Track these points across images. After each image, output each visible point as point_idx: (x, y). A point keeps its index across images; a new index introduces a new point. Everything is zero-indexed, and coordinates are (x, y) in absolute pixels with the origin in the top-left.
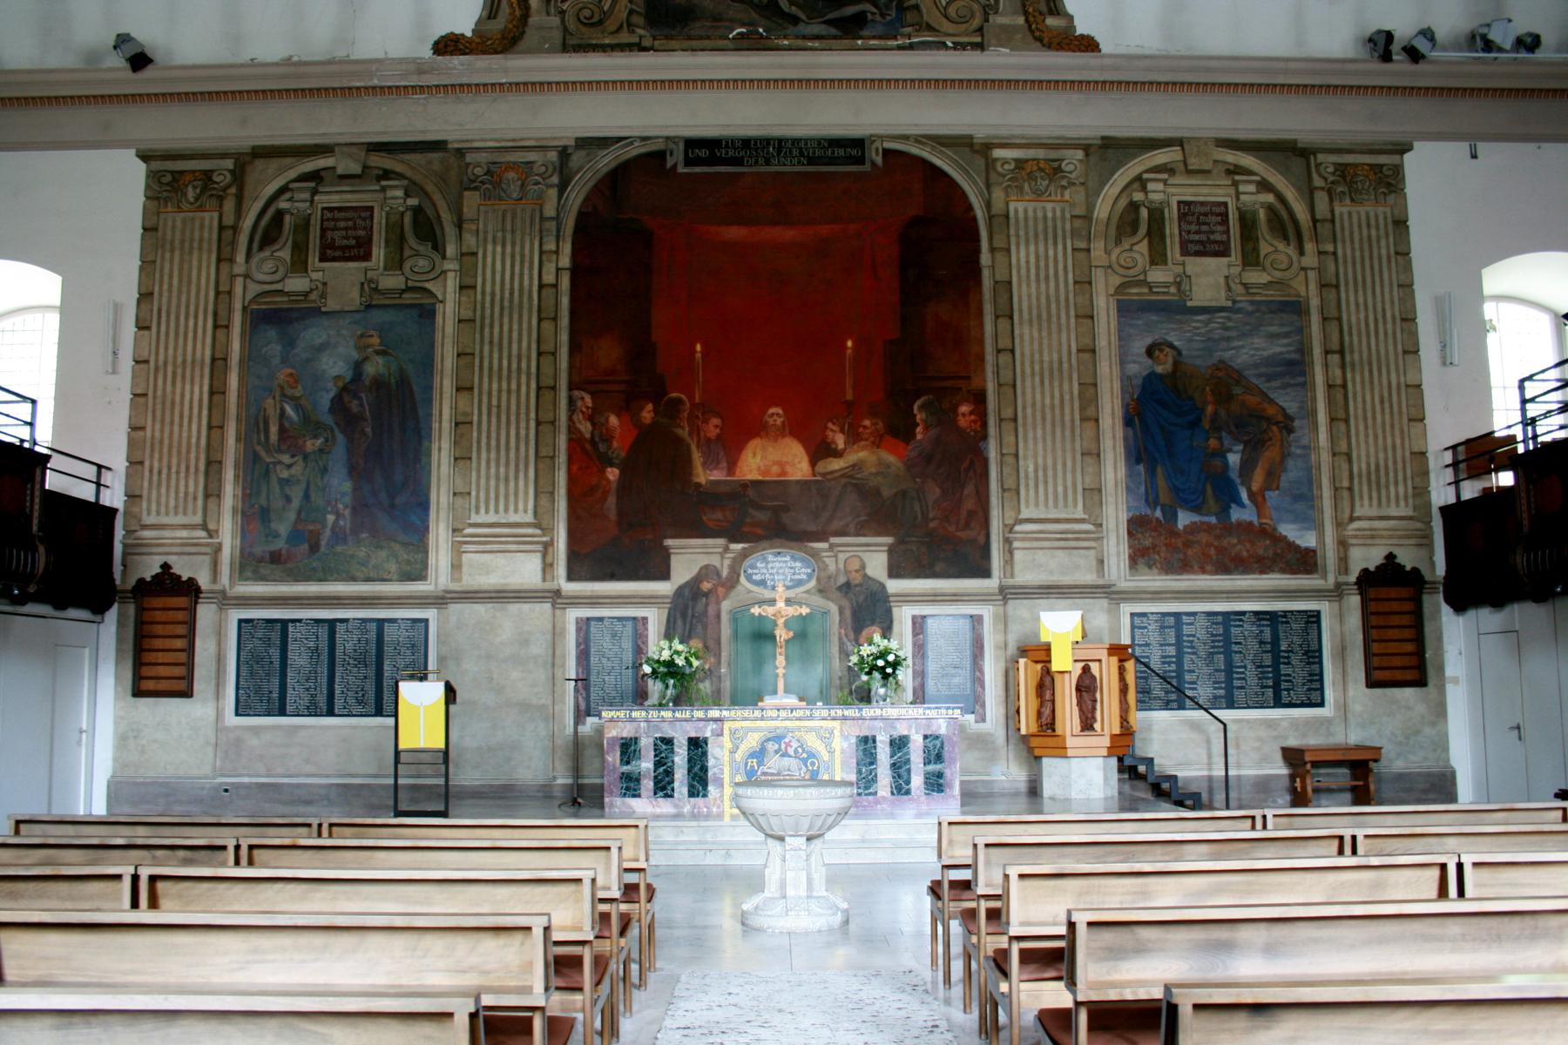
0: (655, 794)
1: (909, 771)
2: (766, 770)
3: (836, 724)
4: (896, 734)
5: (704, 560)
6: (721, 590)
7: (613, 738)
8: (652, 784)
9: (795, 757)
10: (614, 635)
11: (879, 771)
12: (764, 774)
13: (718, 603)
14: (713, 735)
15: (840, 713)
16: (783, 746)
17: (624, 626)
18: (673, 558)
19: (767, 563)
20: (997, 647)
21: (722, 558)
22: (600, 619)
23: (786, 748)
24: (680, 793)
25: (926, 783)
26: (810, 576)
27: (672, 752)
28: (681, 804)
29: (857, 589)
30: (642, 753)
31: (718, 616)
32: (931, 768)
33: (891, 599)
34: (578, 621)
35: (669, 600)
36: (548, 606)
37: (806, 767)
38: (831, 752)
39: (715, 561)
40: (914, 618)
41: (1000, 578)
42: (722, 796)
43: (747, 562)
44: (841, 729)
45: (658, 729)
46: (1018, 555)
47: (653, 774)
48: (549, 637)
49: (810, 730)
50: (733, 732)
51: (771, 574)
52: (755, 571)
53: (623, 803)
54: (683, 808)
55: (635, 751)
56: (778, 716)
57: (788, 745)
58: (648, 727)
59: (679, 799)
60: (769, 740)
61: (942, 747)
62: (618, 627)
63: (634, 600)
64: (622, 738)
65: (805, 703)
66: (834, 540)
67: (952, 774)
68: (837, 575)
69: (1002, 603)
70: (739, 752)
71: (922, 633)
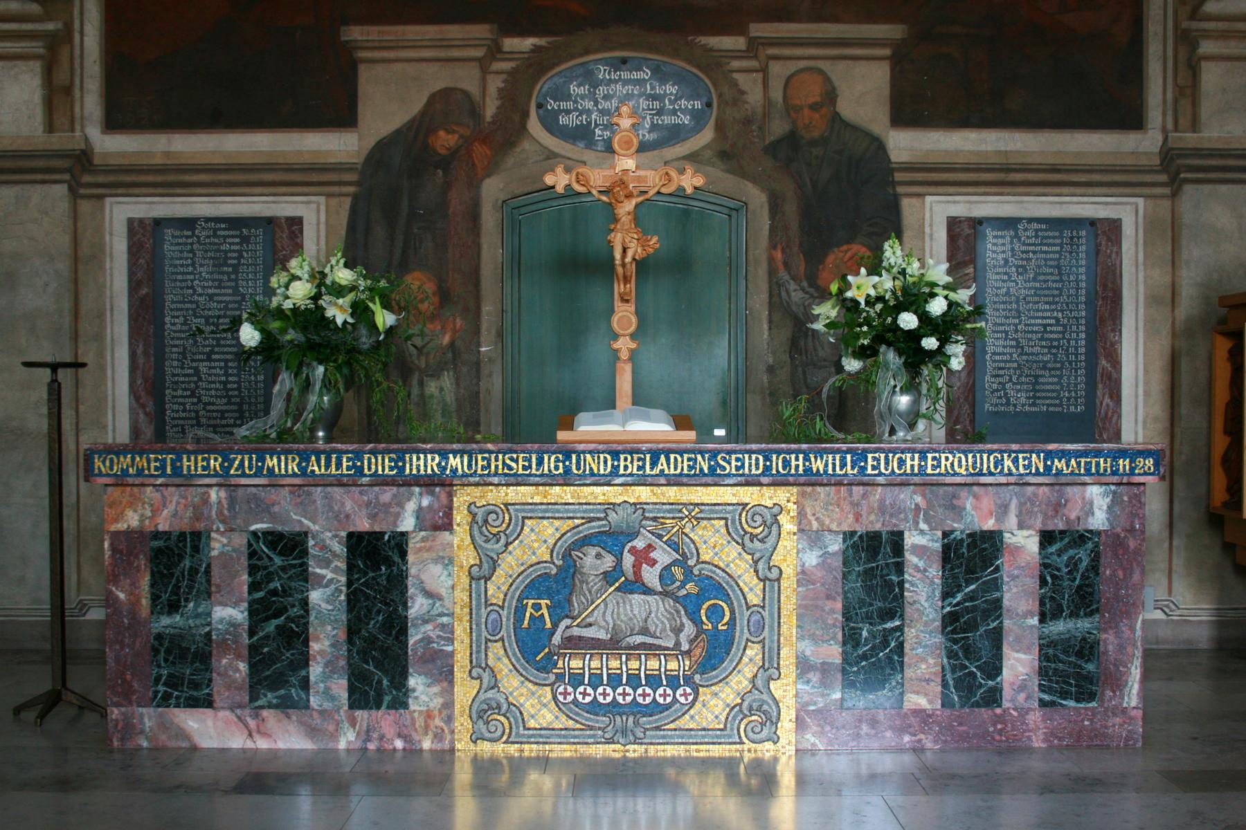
0: (253, 698)
1: (997, 638)
2: (576, 632)
3: (782, 496)
4: (959, 528)
5: (438, 79)
6: (480, 150)
7: (129, 533)
8: (243, 666)
9: (665, 594)
10: (220, 262)
11: (910, 634)
12: (572, 643)
13: (474, 184)
14: (420, 527)
15: (797, 462)
16: (628, 560)
17: (245, 240)
18: (364, 73)
19: (595, 85)
20: (1153, 300)
21: (485, 72)
22: (189, 223)
23: (637, 567)
24: (327, 693)
25: (1042, 672)
26: (699, 118)
27: (304, 575)
28: (331, 728)
29: (817, 151)
30: (216, 579)
31: (474, 216)
32: (1059, 627)
33: (898, 177)
34: (135, 228)
35: (353, 177)
36: (61, 190)
37: (697, 622)
38: (771, 581)
39: (466, 79)
40: (953, 223)
41: (1164, 130)
42: (449, 705)
43: (544, 85)
44: (801, 514)
45: (262, 508)
46: (1211, 75)
47: (246, 640)
48: (63, 266)
49: (701, 513)
50: (480, 521)
51: (603, 112)
52: (563, 105)
53: (163, 725)
54: (334, 736)
55: (194, 571)
56: (615, 472)
57: (644, 557)
58: (232, 501)
59: (322, 713)
60: (585, 541)
61: (1094, 567)
62: (231, 244)
63: (269, 177)
64: (157, 535)
65: (691, 435)
66: (759, 30)
67: (1121, 648)
68: (766, 115)
69: (1167, 191)
71: (973, 261)
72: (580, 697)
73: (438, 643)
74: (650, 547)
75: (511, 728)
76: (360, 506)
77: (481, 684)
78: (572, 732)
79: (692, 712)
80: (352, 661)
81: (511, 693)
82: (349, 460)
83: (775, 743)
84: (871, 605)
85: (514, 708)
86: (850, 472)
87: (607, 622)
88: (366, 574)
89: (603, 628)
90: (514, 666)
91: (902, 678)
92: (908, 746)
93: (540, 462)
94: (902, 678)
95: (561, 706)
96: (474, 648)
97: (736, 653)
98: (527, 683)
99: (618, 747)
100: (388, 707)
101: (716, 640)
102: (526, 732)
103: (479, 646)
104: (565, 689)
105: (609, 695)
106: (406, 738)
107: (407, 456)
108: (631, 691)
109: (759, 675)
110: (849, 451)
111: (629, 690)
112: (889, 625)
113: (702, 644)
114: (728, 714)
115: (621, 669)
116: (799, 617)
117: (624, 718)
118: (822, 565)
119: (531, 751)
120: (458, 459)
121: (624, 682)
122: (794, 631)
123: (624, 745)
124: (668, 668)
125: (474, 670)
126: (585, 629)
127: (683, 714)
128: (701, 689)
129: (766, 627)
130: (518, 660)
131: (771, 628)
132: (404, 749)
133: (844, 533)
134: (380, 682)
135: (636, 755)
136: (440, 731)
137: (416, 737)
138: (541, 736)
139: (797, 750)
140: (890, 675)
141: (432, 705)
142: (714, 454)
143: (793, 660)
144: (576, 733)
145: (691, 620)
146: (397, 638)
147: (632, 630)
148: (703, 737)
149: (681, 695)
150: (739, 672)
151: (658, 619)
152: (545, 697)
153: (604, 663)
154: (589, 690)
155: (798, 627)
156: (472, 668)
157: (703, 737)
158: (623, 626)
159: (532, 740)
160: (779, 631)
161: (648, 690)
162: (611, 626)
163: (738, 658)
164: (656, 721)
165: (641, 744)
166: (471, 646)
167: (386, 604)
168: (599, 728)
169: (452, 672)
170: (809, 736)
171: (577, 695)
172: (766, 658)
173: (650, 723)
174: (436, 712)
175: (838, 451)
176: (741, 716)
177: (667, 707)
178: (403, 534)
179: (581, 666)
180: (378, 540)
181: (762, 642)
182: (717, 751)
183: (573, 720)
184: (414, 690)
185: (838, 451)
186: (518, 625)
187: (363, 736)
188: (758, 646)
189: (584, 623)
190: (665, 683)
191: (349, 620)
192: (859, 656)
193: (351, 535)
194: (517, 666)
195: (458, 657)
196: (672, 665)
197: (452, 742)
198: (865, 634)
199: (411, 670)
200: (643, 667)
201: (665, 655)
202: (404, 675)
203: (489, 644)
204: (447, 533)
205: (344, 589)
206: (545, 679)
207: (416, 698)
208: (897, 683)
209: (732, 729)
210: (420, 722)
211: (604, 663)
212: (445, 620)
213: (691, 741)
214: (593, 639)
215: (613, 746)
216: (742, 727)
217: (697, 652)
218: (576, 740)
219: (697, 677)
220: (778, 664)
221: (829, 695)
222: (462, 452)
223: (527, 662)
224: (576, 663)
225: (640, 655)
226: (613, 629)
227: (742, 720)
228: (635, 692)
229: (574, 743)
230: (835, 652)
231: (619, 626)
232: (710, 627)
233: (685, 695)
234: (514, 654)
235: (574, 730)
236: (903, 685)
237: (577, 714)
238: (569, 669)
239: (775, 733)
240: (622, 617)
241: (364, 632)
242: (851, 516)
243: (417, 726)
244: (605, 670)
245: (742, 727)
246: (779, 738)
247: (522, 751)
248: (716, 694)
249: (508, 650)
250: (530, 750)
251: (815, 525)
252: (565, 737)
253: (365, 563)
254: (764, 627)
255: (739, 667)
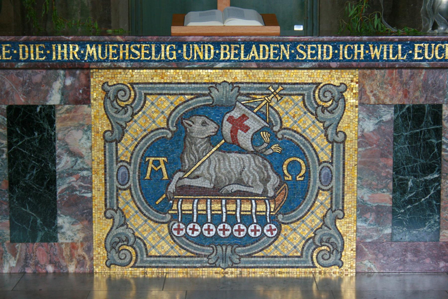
2: (187, 182)
9: (255, 153)
14: (65, 100)
16: (227, 127)
23: (234, 132)
37: (281, 175)
42: (89, 239)
44: (362, 93)
65: (276, 29)
70: (128, 138)
72: (190, 232)
73: (80, 191)
74: (244, 117)
75: (137, 256)
76: (17, 85)
77: (114, 222)
78: (184, 259)
79: (276, 243)
80: (12, 206)
81: (137, 229)
82: (7, 48)
83: (340, 267)
84: (416, 162)
85: (139, 241)
86: (400, 58)
87: (210, 175)
88: (22, 138)
89: (208, 179)
90: (139, 208)
91: (439, 218)
92: (443, 270)
93: (158, 51)
94: (439, 218)
95: (176, 239)
96: (108, 195)
97: (310, 199)
98: (149, 221)
99: (219, 269)
100: (41, 241)
101: (295, 188)
102: (148, 259)
103: (111, 193)
104: (179, 226)
105: (212, 230)
106: (55, 264)
107: (54, 46)
108: (229, 228)
109: (328, 215)
110: (400, 42)
111: (227, 226)
112: (430, 177)
113: (284, 191)
114: (304, 245)
115: (221, 210)
116: (360, 171)
117: (224, 248)
118: (377, 131)
119: (153, 273)
120: (94, 49)
121: (224, 220)
122: (355, 181)
123: (224, 269)
124: (258, 209)
125: (108, 212)
126: (193, 180)
127: (270, 245)
128: (283, 226)
129: (334, 178)
130: (142, 204)
131: (338, 179)
132: (54, 272)
133: (396, 106)
134: (35, 221)
135: (233, 276)
136: (82, 259)
137: (64, 264)
138: (160, 262)
139: (357, 273)
140: (430, 215)
141: (75, 239)
142: (294, 44)
143: (354, 204)
144: (187, 259)
145: (276, 173)
146: (48, 187)
147: (230, 180)
148: (285, 262)
149: (268, 231)
150: (312, 213)
151: (250, 172)
152: (163, 232)
153: (209, 206)
154: (197, 227)
155: (358, 178)
156: (107, 210)
157: (285, 262)
158: (223, 178)
159: (154, 265)
160: (344, 181)
161: (242, 227)
162: (214, 178)
163: (312, 202)
164: (248, 250)
165: (237, 267)
166: (106, 193)
167: (39, 161)
168: (205, 256)
169: (91, 213)
170: (366, 262)
171: (188, 231)
172: (334, 202)
173: (244, 251)
174: (79, 244)
175: (392, 42)
176: (314, 246)
177: (259, 239)
178: (51, 107)
179: (191, 208)
180: (31, 111)
181: (331, 190)
182: (295, 273)
183: (185, 249)
184: (61, 227)
185: (392, 42)
186: (142, 177)
187: (22, 263)
188: (327, 193)
189: (193, 176)
190: (255, 221)
191: (10, 174)
192: (405, 201)
193: (10, 108)
194: (142, 208)
195: (95, 202)
196: (261, 207)
197: (92, 266)
198: (410, 184)
199: (59, 212)
200: (238, 209)
201: (255, 200)
202: (54, 216)
203: (120, 192)
204: (86, 106)
205: (5, 149)
206: (163, 218)
207: (63, 233)
208: (435, 221)
209: (307, 257)
210: (66, 252)
211: (209, 206)
212: (85, 173)
213: (275, 265)
214: (200, 187)
215: (215, 269)
216: (315, 254)
217: (280, 197)
218: (187, 265)
219: (280, 217)
220: (343, 207)
221: (382, 230)
222: (97, 43)
223: (149, 206)
224: (187, 206)
225: (236, 200)
226: (215, 180)
227: (315, 249)
228: (232, 228)
229: (186, 267)
230: (387, 198)
231: (220, 177)
232: (290, 178)
233: (271, 230)
234: (139, 199)
235: (185, 257)
236: (439, 223)
237: (188, 245)
238: (182, 210)
239: (340, 259)
240: (222, 170)
241: (22, 183)
242: (401, 93)
243: (64, 255)
244: (209, 211)
245: (315, 254)
246: (343, 263)
247: (145, 273)
248: (295, 230)
249: (135, 196)
250: (152, 272)
251: (373, 100)
252: (178, 262)
253: (22, 130)
254: (332, 179)
255: (313, 209)
